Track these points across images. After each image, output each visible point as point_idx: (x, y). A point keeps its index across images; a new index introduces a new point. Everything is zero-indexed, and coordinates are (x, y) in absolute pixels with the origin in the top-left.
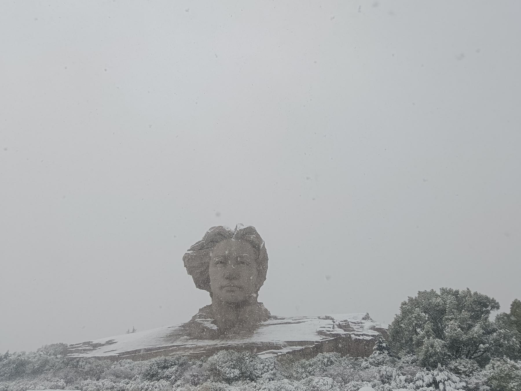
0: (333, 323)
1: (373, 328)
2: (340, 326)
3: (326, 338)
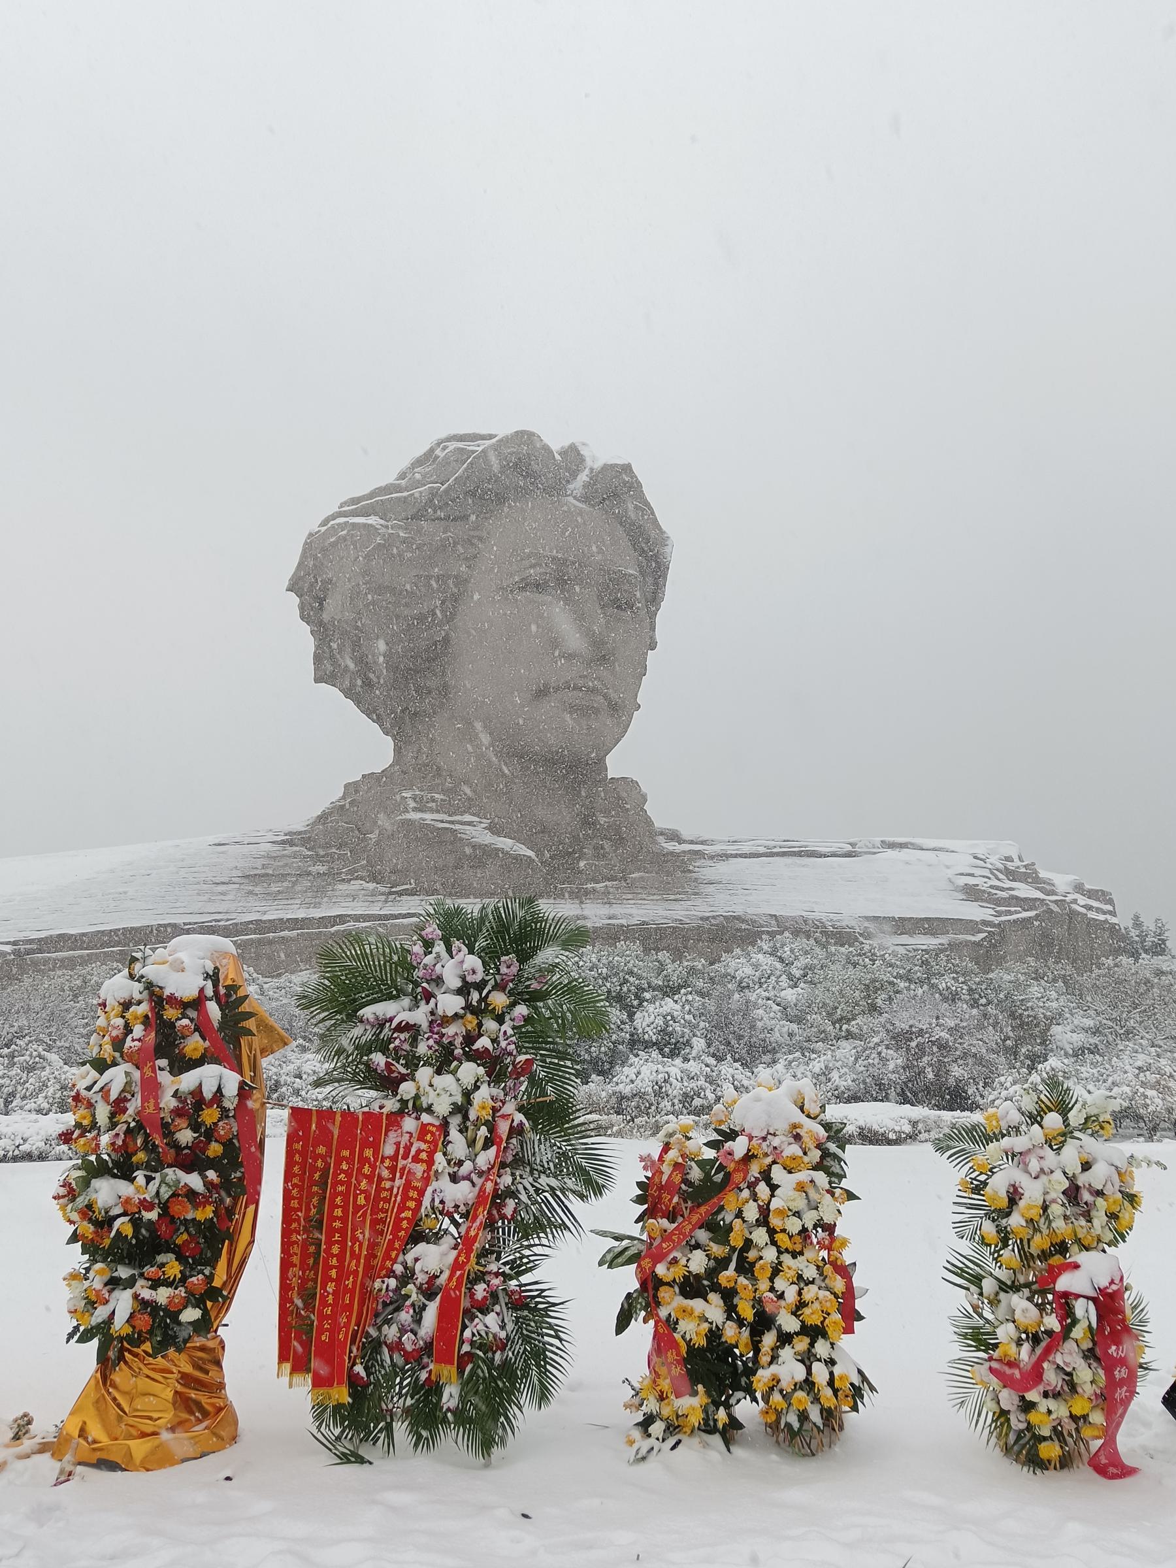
0: (981, 863)
1: (1079, 888)
2: (1012, 875)
3: (1010, 913)
